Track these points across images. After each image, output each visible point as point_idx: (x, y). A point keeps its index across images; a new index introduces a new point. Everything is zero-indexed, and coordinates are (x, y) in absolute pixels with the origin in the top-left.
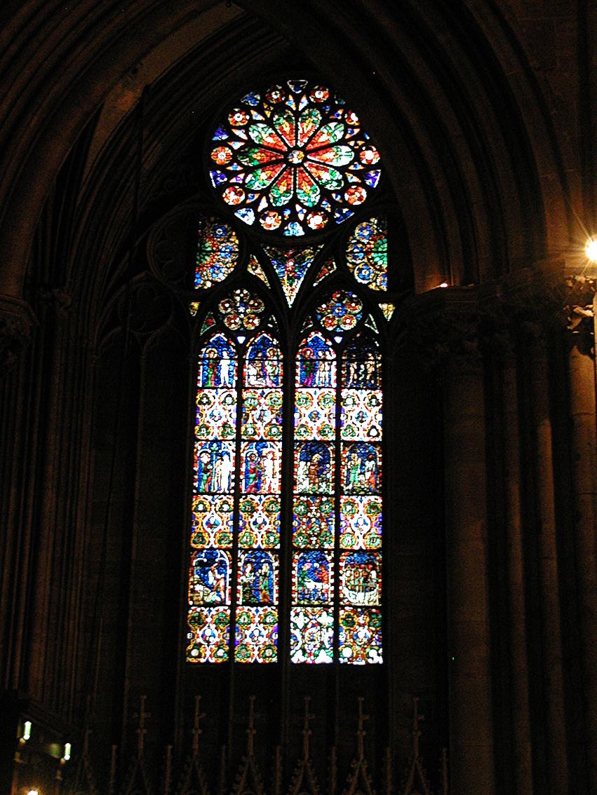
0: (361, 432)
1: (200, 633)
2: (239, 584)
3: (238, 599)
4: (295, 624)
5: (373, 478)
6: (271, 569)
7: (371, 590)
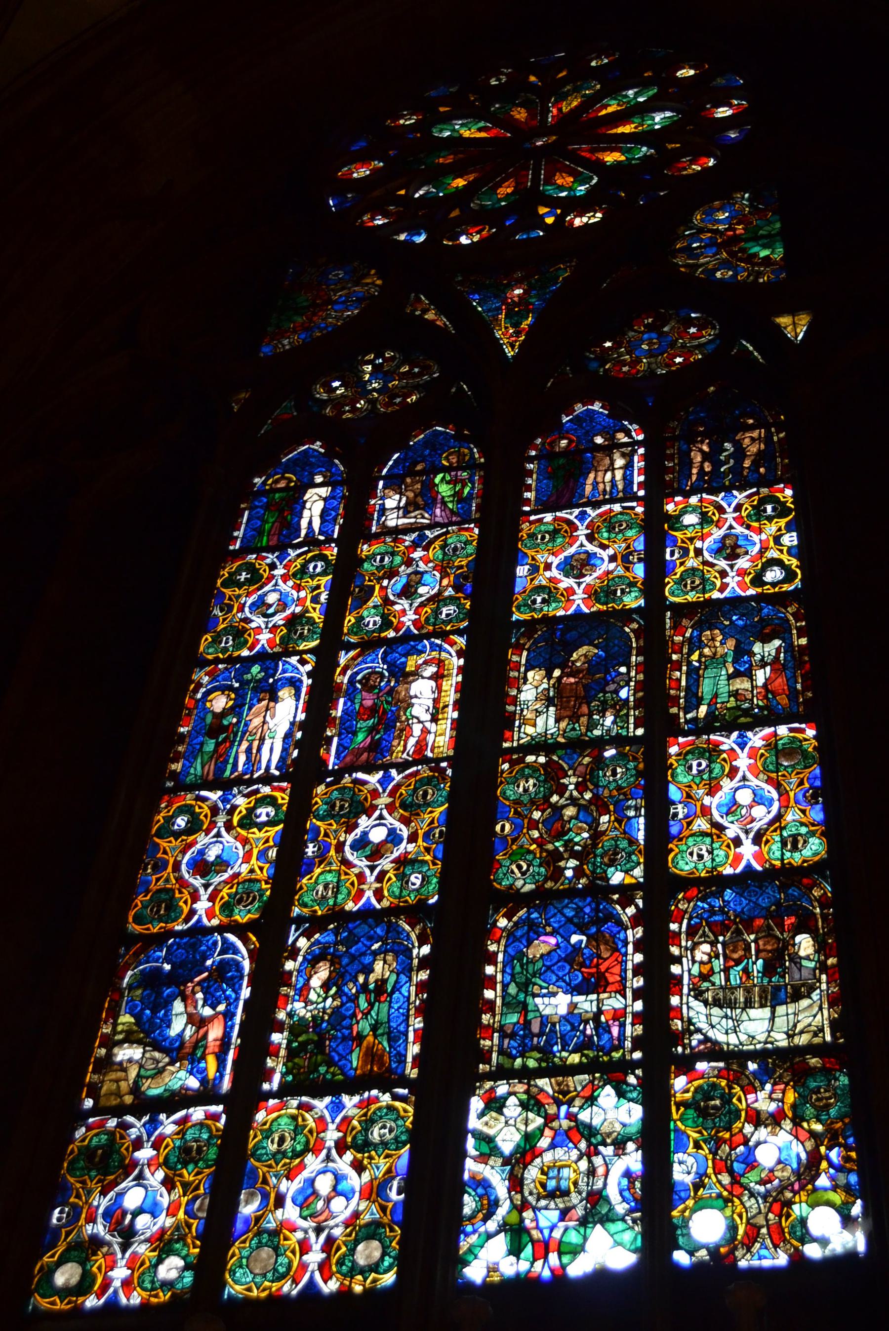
0: (732, 581)
1: (103, 1203)
2: (279, 1027)
3: (268, 1075)
4: (488, 1140)
5: (780, 682)
6: (407, 970)
7: (796, 997)
